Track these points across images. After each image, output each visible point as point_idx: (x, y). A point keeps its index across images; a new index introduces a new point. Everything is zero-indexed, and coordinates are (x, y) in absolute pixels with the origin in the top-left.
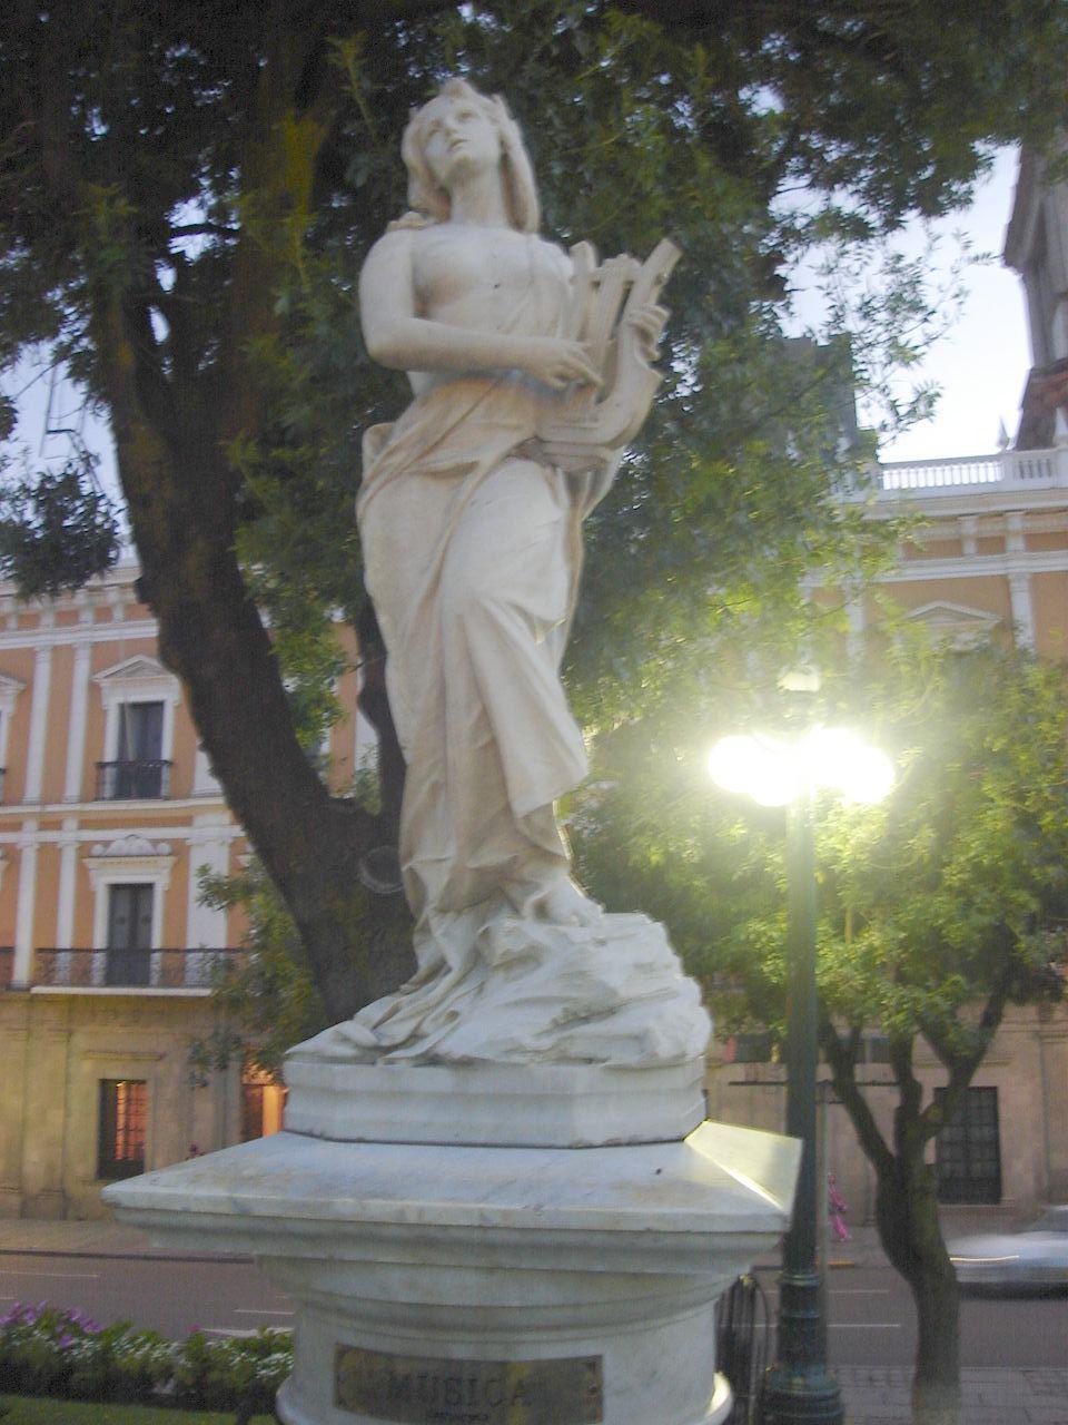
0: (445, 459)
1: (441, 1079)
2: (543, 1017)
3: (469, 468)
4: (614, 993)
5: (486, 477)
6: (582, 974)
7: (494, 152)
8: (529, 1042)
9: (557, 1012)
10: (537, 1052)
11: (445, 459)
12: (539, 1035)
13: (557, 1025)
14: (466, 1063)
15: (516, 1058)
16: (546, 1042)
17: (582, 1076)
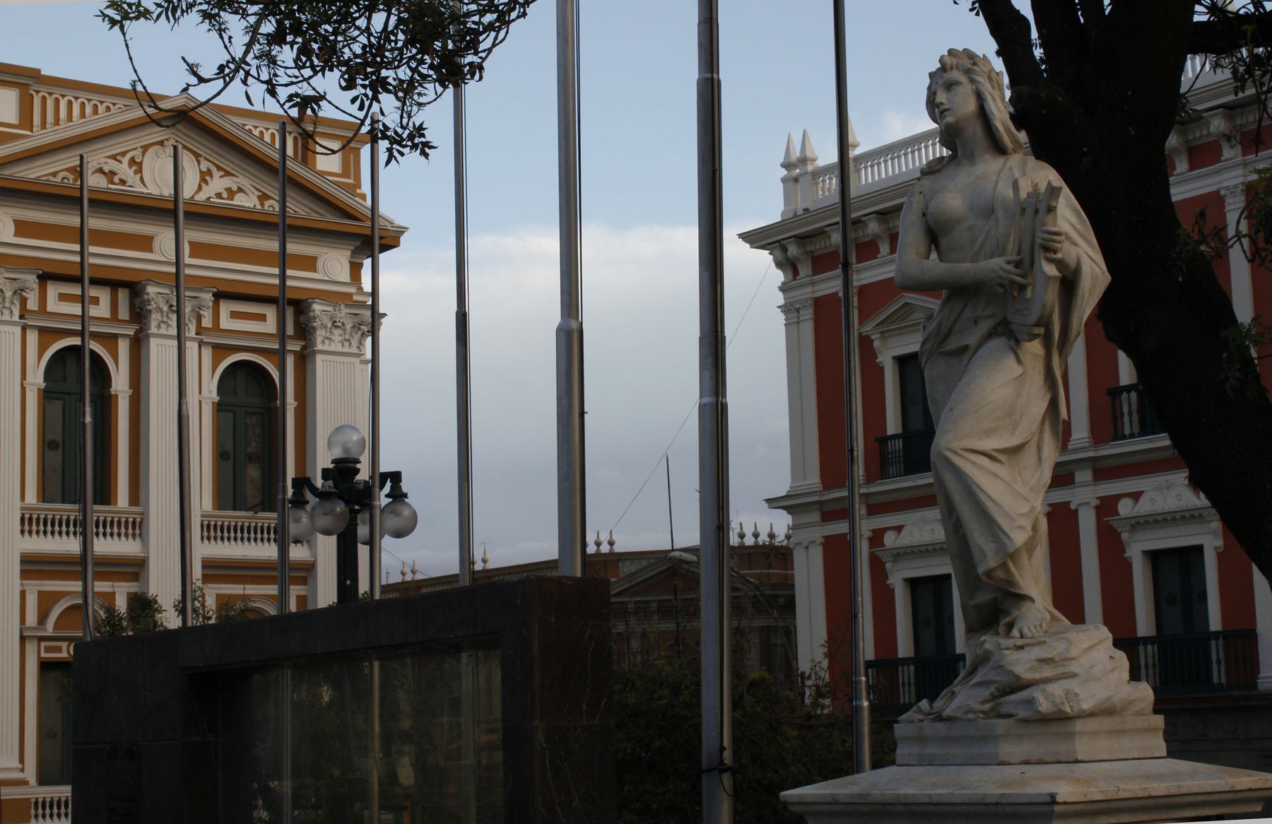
0: (952, 345)
1: (941, 728)
2: (985, 693)
3: (966, 348)
4: (1018, 678)
5: (976, 352)
6: (1001, 667)
7: (971, 106)
8: (978, 707)
9: (992, 689)
10: (982, 712)
11: (952, 345)
12: (983, 703)
13: (994, 697)
14: (950, 719)
15: (971, 716)
16: (987, 707)
17: (1001, 725)
